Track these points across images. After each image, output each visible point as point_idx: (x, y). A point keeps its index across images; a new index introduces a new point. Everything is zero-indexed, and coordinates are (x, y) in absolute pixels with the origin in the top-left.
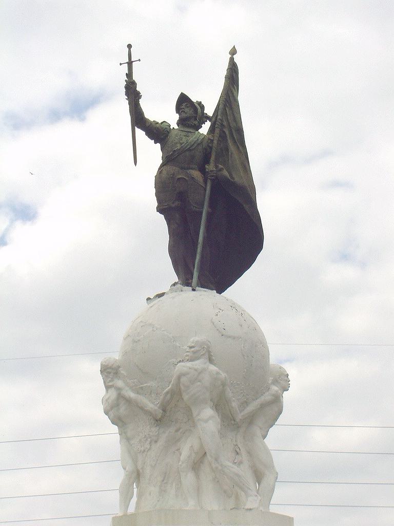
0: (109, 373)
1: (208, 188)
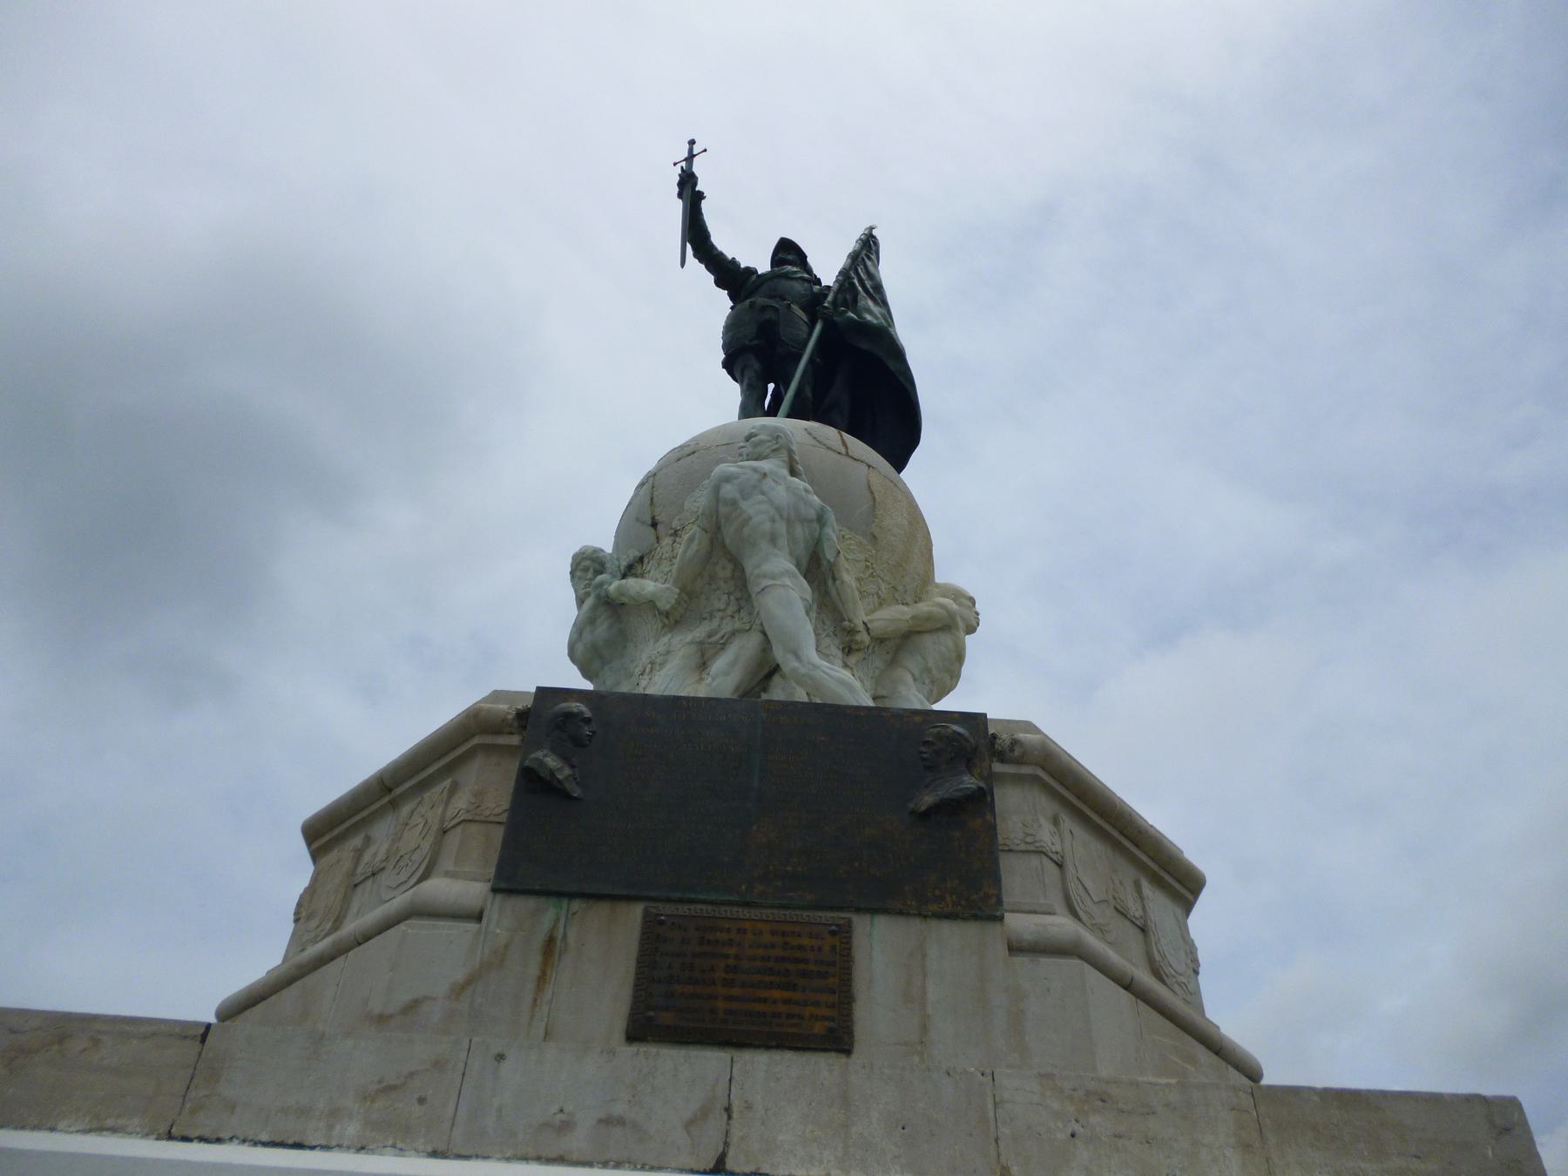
0: (586, 570)
1: (818, 327)
